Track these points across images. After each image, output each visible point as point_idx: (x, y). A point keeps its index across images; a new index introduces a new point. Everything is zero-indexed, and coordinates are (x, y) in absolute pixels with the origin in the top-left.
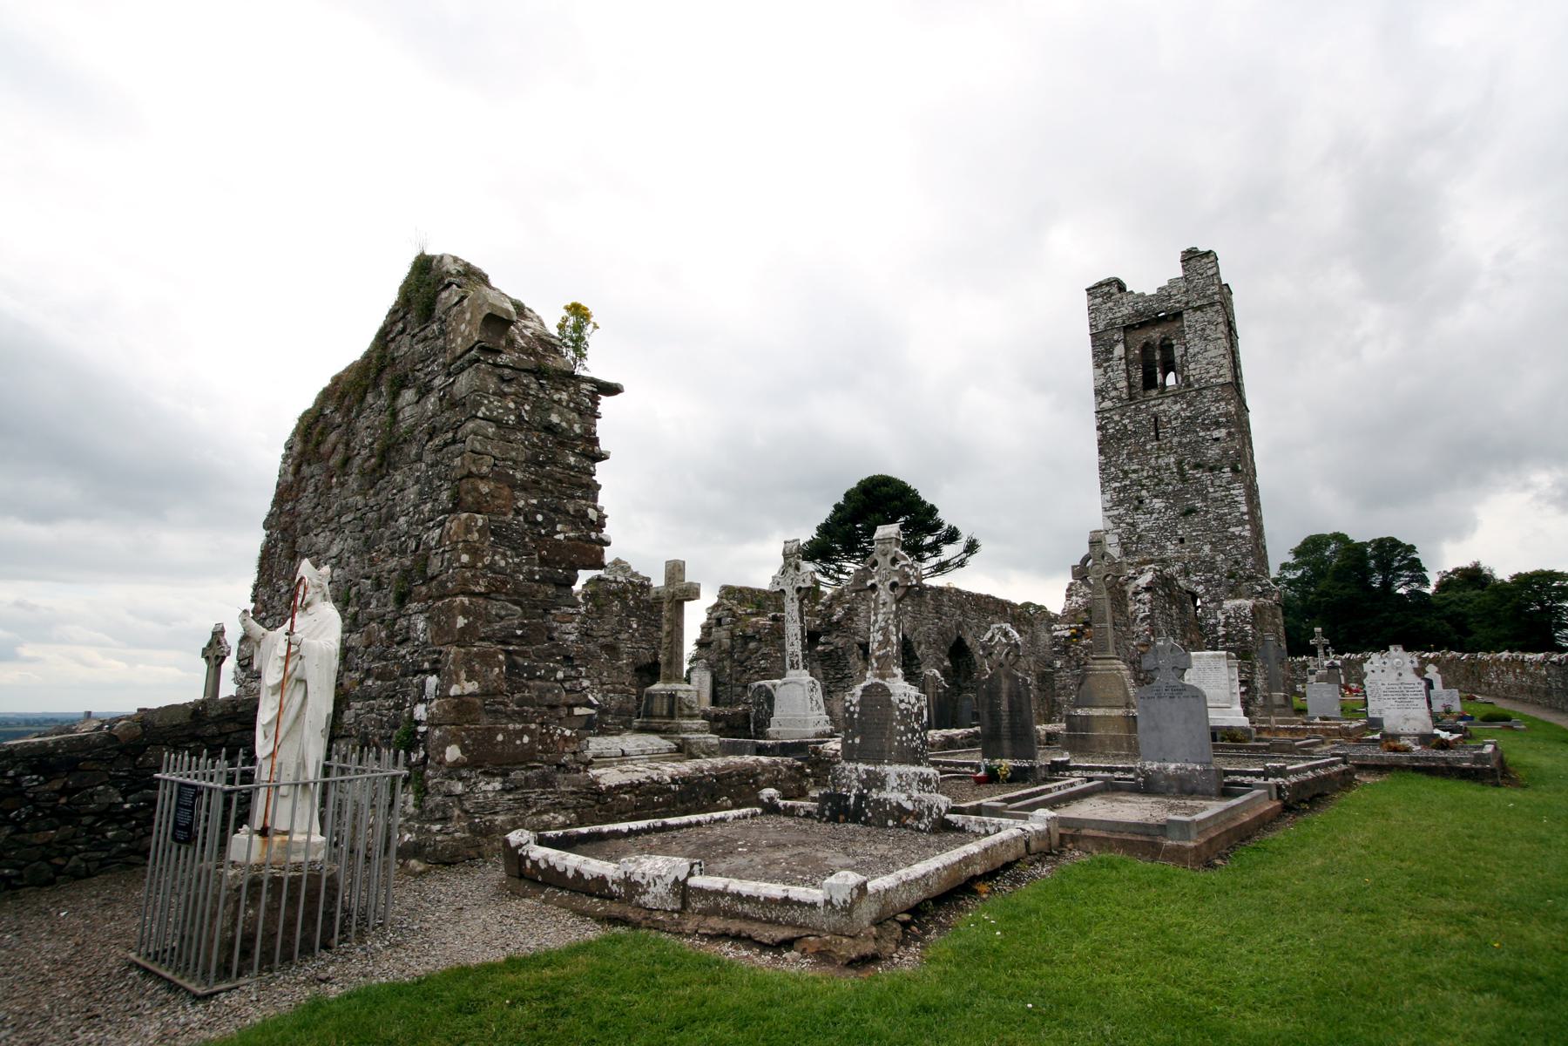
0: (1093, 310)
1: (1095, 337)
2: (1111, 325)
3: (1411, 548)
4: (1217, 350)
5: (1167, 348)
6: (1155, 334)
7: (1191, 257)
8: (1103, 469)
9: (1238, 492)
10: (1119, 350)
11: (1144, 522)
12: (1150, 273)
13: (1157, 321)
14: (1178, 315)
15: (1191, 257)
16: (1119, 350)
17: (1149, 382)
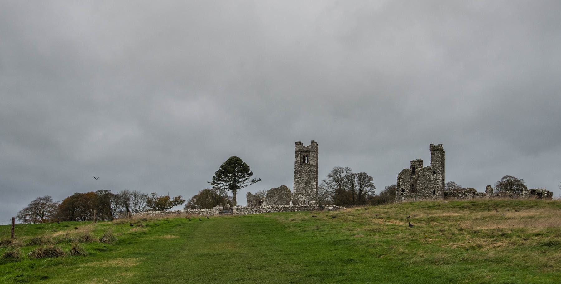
0: (296, 147)
1: (296, 152)
2: (299, 150)
3: (371, 178)
4: (315, 160)
5: (307, 156)
6: (306, 154)
7: (313, 142)
8: (295, 176)
9: (315, 183)
10: (299, 155)
11: (300, 187)
12: (307, 144)
13: (307, 152)
14: (310, 152)
15: (313, 142)
16: (299, 155)
17: (304, 162)
